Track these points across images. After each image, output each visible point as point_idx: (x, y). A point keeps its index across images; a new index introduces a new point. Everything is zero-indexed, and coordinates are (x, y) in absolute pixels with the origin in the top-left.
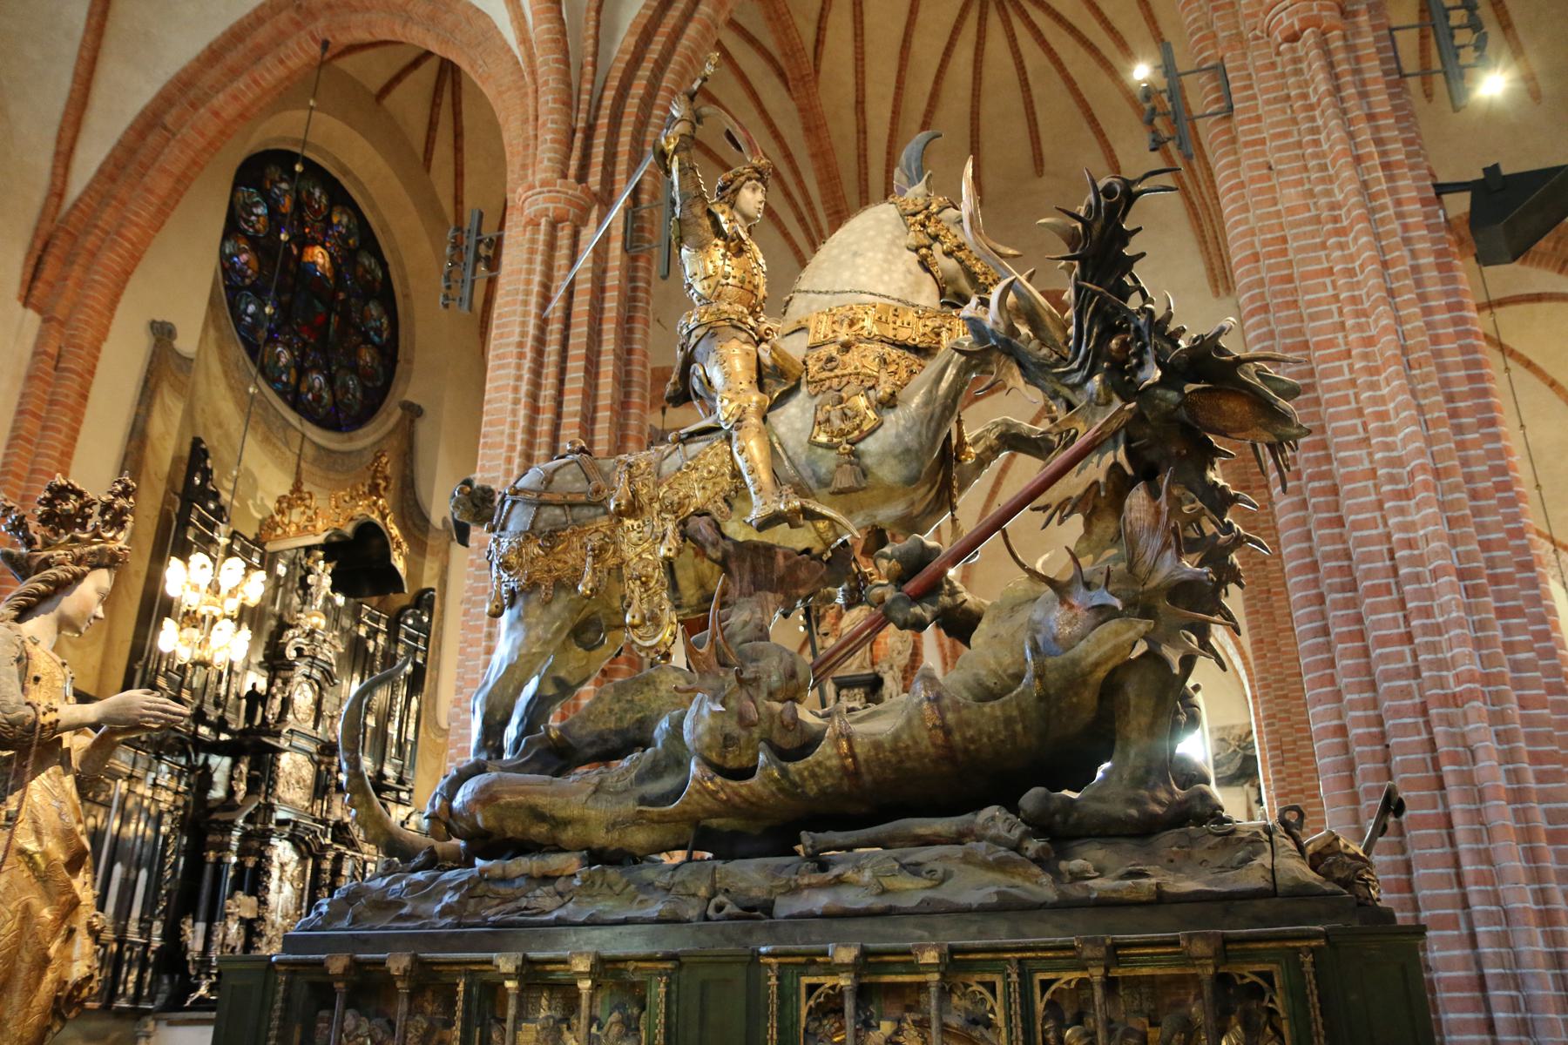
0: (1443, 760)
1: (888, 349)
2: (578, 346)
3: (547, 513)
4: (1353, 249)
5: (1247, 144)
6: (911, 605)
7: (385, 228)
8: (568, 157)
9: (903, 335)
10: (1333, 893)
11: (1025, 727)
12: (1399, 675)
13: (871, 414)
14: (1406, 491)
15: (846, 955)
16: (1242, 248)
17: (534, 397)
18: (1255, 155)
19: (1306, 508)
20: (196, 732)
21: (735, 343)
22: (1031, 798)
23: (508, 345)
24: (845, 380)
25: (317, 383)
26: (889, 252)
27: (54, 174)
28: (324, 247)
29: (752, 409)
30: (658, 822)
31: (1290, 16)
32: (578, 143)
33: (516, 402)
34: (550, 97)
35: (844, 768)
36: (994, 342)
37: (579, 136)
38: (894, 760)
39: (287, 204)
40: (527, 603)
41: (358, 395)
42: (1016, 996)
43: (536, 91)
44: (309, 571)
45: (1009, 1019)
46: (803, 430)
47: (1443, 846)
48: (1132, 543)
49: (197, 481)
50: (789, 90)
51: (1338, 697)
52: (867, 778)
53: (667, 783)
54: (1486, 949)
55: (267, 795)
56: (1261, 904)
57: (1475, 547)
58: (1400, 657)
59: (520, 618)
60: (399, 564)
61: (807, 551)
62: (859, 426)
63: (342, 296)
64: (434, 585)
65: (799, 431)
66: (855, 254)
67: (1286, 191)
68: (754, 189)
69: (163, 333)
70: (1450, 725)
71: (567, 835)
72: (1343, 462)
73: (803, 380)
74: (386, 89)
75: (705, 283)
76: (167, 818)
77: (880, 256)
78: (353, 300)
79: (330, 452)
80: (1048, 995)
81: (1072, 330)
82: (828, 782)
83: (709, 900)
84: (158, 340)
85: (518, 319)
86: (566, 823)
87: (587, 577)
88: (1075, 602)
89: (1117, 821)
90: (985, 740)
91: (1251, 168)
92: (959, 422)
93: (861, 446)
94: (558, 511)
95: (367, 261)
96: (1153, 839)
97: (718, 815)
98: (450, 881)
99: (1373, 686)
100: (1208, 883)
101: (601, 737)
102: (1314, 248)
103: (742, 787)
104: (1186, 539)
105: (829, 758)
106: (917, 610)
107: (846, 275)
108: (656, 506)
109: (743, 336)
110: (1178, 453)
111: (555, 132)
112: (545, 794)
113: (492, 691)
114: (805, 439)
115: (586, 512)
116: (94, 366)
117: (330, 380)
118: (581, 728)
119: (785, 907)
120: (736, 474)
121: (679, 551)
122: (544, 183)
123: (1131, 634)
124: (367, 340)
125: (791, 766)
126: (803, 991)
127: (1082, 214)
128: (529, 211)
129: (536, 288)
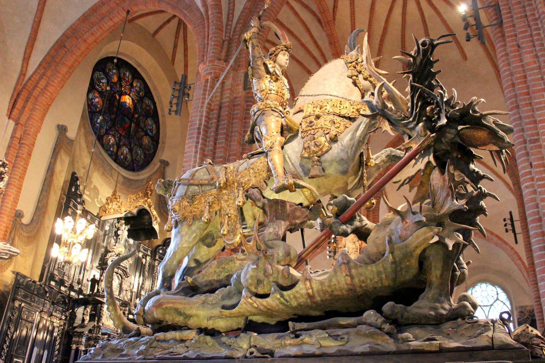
1: (336, 117)
2: (223, 129)
3: (192, 188)
5: (509, 37)
6: (341, 225)
7: (155, 88)
9: (343, 112)
10: (519, 348)
11: (386, 276)
13: (327, 144)
16: (507, 81)
18: (512, 41)
19: (536, 194)
20: (69, 294)
21: (272, 117)
22: (388, 307)
23: (194, 129)
24: (316, 130)
25: (125, 152)
27: (22, 67)
28: (129, 95)
29: (277, 143)
30: (230, 317)
32: (225, 46)
33: (196, 152)
35: (308, 294)
37: (226, 43)
38: (329, 290)
39: (115, 79)
40: (182, 226)
41: (142, 157)
44: (118, 229)
49: (73, 190)
50: (322, 27)
55: (98, 322)
56: (486, 352)
59: (179, 232)
60: (156, 227)
61: (301, 204)
63: (136, 116)
65: (297, 152)
66: (325, 79)
67: (525, 56)
68: (284, 55)
69: (62, 130)
71: (192, 322)
74: (156, 32)
76: (56, 330)
78: (141, 118)
79: (129, 180)
81: (409, 104)
82: (301, 300)
84: (60, 132)
85: (198, 118)
89: (426, 317)
90: (369, 281)
91: (511, 47)
93: (323, 158)
94: (196, 188)
95: (147, 101)
96: (441, 325)
97: (254, 315)
98: (143, 341)
100: (463, 344)
101: (211, 283)
102: (538, 79)
103: (264, 301)
104: (458, 193)
105: (301, 289)
106: (344, 227)
109: (276, 114)
110: (457, 157)
112: (181, 303)
115: (208, 188)
116: (34, 142)
117: (131, 150)
118: (202, 279)
120: (269, 170)
121: (244, 203)
123: (431, 233)
124: (147, 134)
125: (285, 293)
127: (413, 54)
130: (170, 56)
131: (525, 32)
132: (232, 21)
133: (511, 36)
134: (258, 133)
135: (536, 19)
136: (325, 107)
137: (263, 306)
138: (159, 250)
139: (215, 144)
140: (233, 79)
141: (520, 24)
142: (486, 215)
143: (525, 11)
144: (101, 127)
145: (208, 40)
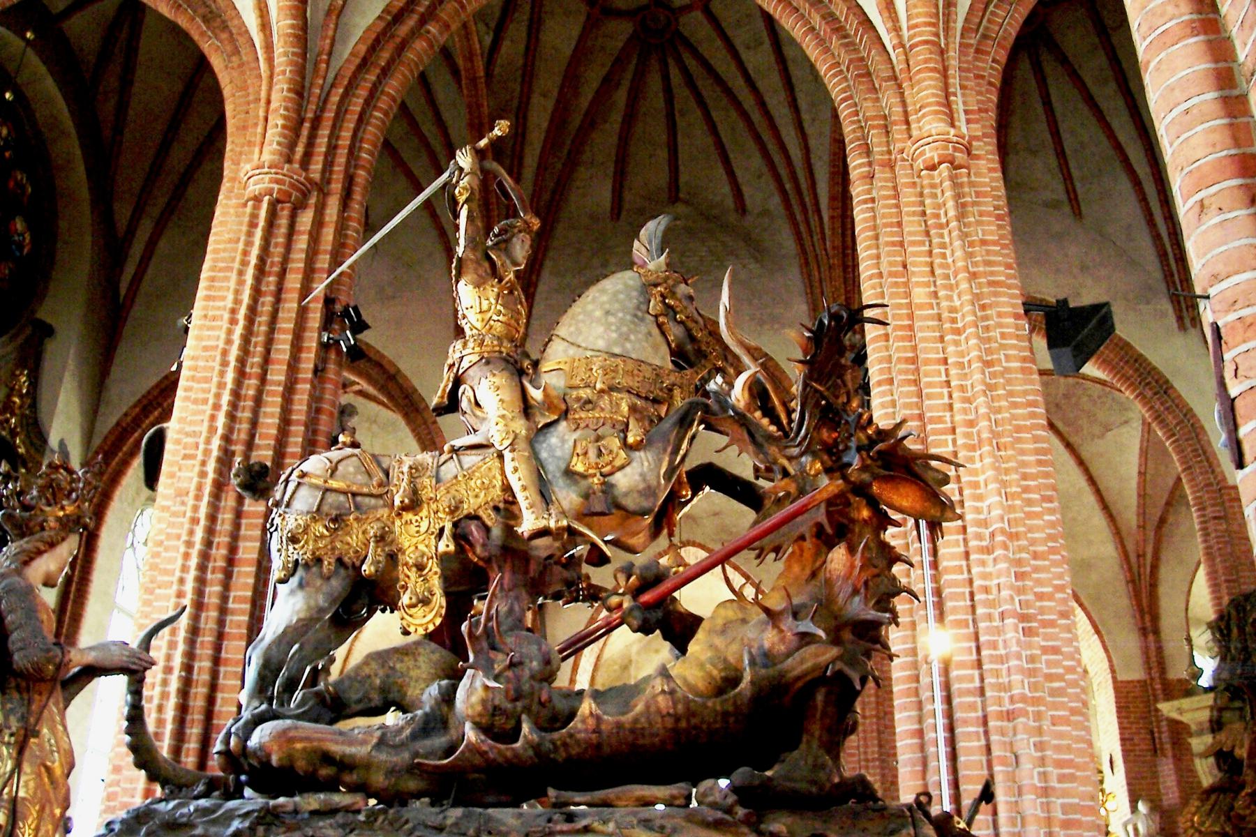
0: (995, 762)
3: (331, 498)
4: (963, 347)
12: (969, 692)
14: (987, 547)
31: (931, 150)
32: (305, 132)
34: (285, 86)
37: (307, 125)
43: (271, 77)
47: (988, 828)
52: (606, 749)
53: (439, 741)
57: (1031, 597)
58: (972, 680)
59: (301, 585)
66: (608, 313)
70: (1003, 735)
75: (479, 317)
81: (796, 416)
82: (574, 751)
85: (232, 284)
88: (783, 627)
94: (342, 498)
105: (580, 732)
108: (434, 506)
111: (285, 118)
113: (269, 647)
114: (563, 466)
120: (507, 488)
128: (254, 188)
131: (922, 243)
132: (325, 78)
134: (469, 401)
135: (941, 226)
137: (505, 757)
143: (922, 204)
145: (267, 111)
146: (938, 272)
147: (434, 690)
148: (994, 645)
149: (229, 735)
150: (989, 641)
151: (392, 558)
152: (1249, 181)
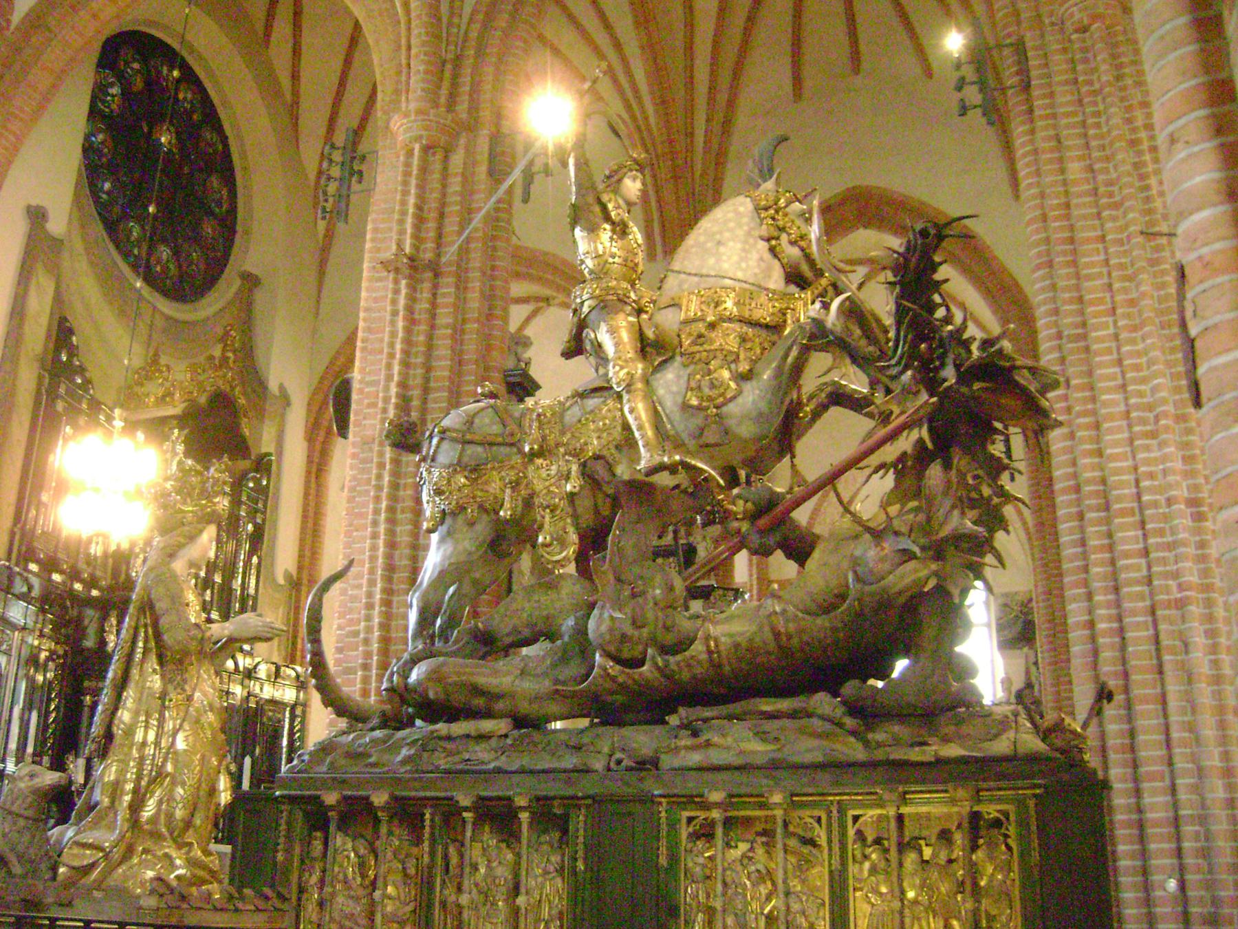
3: (470, 450)
8: (440, 87)
13: (732, 384)
15: (716, 796)
17: (410, 310)
20: (72, 589)
21: (621, 316)
22: (850, 688)
25: (165, 256)
26: (746, 242)
32: (447, 75)
33: (395, 313)
34: (423, 31)
36: (831, 337)
39: (139, 84)
41: (202, 267)
42: (835, 826)
43: (409, 22)
45: (830, 842)
46: (678, 393)
48: (930, 502)
51: (1090, 596)
52: (727, 668)
54: (1183, 796)
62: (722, 395)
64: (271, 449)
66: (719, 243)
68: (634, 179)
70: (1171, 624)
72: (1105, 404)
73: (678, 350)
77: (739, 246)
80: (857, 825)
81: (892, 335)
82: (698, 670)
83: (611, 756)
84: (33, 224)
86: (500, 696)
87: (507, 505)
92: (799, 389)
93: (725, 409)
94: (479, 449)
95: (208, 135)
97: (616, 693)
98: (404, 739)
99: (1116, 590)
107: (712, 261)
108: (562, 450)
114: (680, 400)
117: (176, 254)
119: (666, 761)
120: (626, 427)
122: (420, 112)
125: (671, 659)
126: (684, 821)
129: (411, 210)
130: (260, 28)
131: (1075, 113)
133: (1047, 117)
136: (724, 306)
138: (248, 480)
139: (434, 295)
140: (467, 149)
141: (1064, 98)
142: (1008, 532)
143: (1074, 70)
144: (112, 203)
145: (409, 57)
146: (1093, 143)
147: (571, 622)
148: (1161, 532)
149: (392, 675)
150: (1154, 529)
151: (528, 503)
152: (1216, 110)
